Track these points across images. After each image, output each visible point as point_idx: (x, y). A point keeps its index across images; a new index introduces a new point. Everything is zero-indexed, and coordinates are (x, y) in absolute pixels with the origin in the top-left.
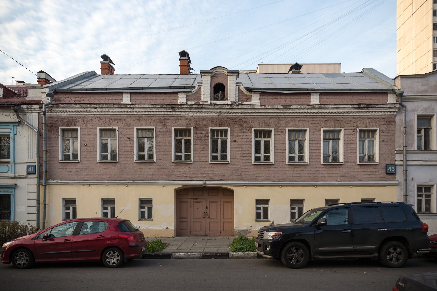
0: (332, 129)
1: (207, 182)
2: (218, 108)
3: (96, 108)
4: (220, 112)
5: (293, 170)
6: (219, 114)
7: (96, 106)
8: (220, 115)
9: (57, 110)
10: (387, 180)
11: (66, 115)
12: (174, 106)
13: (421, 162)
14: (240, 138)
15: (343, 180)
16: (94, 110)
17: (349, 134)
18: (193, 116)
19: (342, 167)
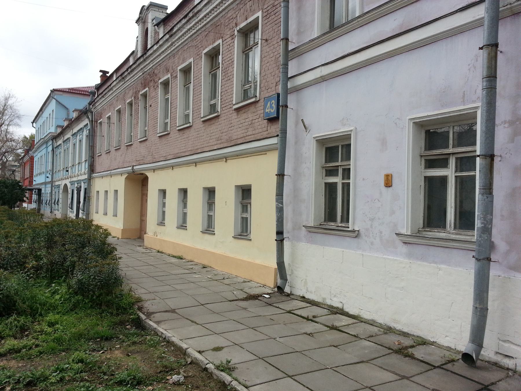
0: (211, 47)
1: (135, 168)
2: (139, 65)
3: (103, 97)
4: (142, 69)
5: (183, 137)
6: (142, 73)
7: (102, 95)
8: (143, 73)
9: (97, 105)
10: (268, 136)
11: (100, 109)
12: (123, 76)
13: (321, 72)
14: (153, 100)
15: (219, 147)
16: (104, 99)
17: (228, 47)
18: (134, 83)
19: (220, 120)
